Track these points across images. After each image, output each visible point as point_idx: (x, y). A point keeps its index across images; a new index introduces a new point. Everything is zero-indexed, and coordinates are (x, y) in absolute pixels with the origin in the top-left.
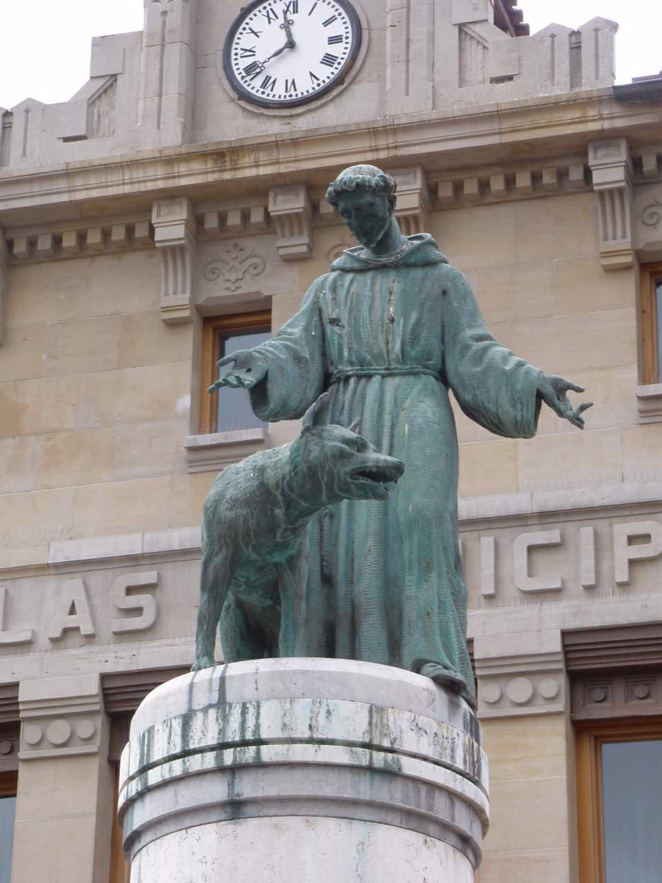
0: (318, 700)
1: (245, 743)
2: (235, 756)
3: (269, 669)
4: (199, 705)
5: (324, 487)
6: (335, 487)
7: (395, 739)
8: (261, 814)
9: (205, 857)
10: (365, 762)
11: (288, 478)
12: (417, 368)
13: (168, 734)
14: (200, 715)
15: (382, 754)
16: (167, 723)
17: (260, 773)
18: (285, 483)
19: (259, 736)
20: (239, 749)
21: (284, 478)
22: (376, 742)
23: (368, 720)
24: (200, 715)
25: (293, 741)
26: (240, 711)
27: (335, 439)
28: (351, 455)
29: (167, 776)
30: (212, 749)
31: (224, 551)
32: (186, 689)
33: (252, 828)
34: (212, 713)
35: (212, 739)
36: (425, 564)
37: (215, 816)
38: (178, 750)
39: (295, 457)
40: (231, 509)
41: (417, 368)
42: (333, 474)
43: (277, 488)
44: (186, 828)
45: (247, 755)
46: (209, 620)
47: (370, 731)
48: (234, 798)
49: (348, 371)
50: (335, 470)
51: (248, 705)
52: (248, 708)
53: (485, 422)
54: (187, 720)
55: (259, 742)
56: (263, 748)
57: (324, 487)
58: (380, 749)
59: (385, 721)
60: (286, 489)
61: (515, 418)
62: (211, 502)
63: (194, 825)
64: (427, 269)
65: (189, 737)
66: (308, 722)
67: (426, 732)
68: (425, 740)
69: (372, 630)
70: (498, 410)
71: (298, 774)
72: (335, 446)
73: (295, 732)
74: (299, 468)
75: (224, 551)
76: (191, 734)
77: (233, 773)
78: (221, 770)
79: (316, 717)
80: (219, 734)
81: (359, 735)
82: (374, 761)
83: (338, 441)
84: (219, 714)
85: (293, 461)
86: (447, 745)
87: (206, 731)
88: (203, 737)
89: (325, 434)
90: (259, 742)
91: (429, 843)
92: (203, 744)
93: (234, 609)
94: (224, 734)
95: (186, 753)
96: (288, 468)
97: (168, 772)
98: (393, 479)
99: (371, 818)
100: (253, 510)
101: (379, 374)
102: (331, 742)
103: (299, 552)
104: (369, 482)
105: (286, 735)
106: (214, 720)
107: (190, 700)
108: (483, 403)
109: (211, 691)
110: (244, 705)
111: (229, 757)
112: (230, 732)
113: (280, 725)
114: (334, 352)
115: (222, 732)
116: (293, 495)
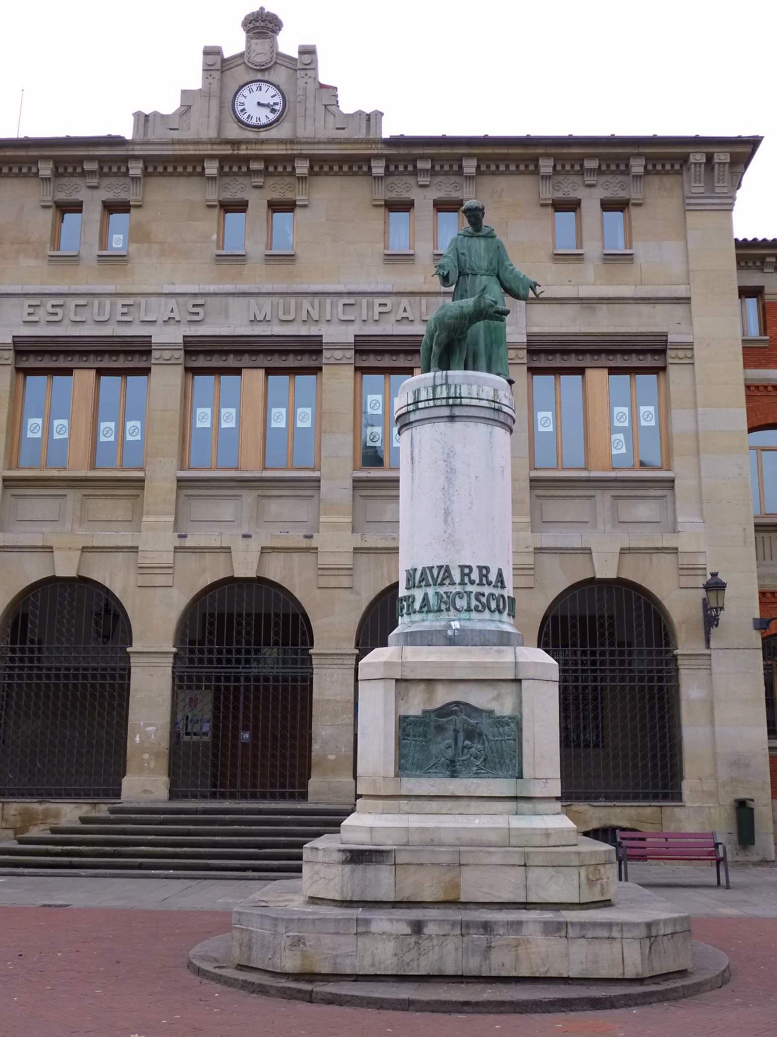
14: (439, 388)
24: (439, 388)
33: (458, 425)
34: (444, 387)
35: (445, 395)
37: (444, 420)
54: (434, 387)
55: (461, 398)
69: (483, 361)
71: (473, 409)
78: (448, 405)
81: (491, 398)
87: (442, 392)
90: (461, 398)
95: (434, 399)
111: (451, 401)
114: (463, 264)
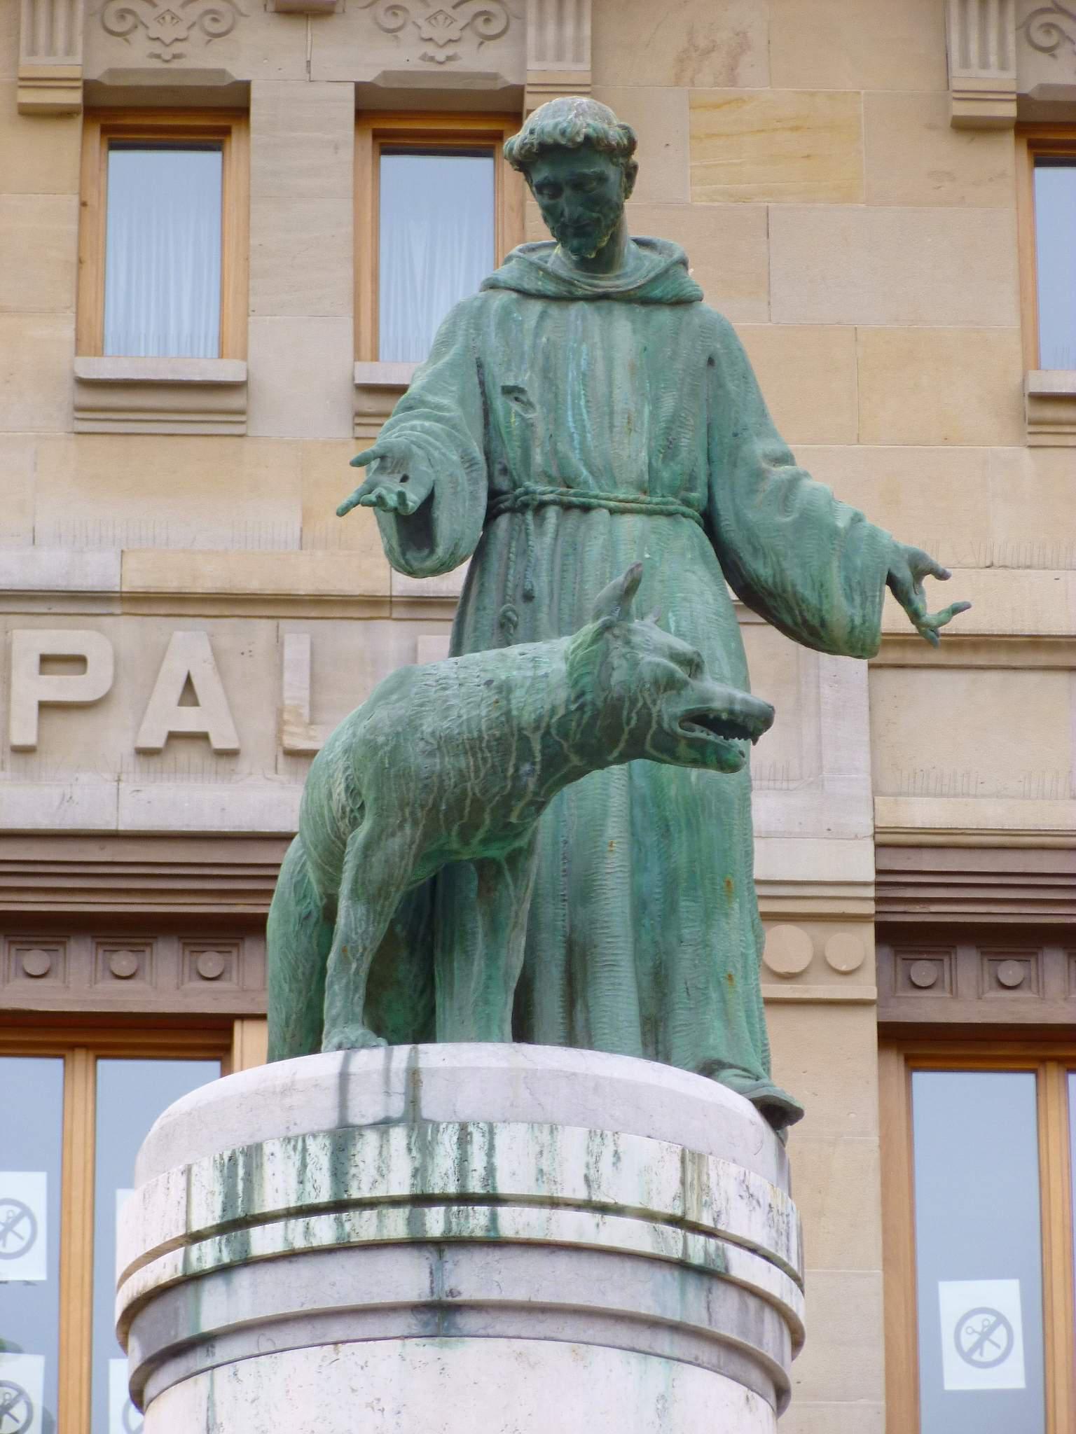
0: (599, 1132)
1: (465, 1199)
2: (448, 1222)
3: (504, 1064)
4: (363, 1116)
5: (625, 736)
6: (649, 737)
7: (719, 1214)
8: (490, 1332)
9: (379, 1400)
10: (677, 1254)
11: (561, 712)
12: (672, 503)
13: (298, 1164)
14: (371, 1138)
15: (702, 1238)
16: (297, 1143)
17: (494, 1256)
18: (554, 720)
19: (494, 1188)
20: (455, 1208)
21: (553, 710)
22: (692, 1217)
23: (678, 1175)
24: (371, 1138)
25: (554, 1203)
26: (455, 1139)
27: (657, 650)
28: (686, 684)
29: (300, 1244)
30: (395, 1202)
31: (408, 829)
32: (333, 1082)
33: (475, 1357)
34: (398, 1136)
35: (400, 1185)
36: (724, 884)
37: (400, 1324)
38: (324, 1196)
39: (581, 676)
40: (431, 754)
41: (672, 503)
42: (650, 715)
43: (537, 728)
44: (336, 1343)
45: (472, 1223)
46: (362, 955)
47: (683, 1196)
48: (444, 1298)
49: (543, 493)
50: (654, 710)
51: (471, 1129)
52: (470, 1134)
53: (788, 620)
54: (343, 1140)
55: (493, 1200)
56: (502, 1211)
57: (625, 736)
58: (696, 1228)
59: (705, 1178)
60: (553, 732)
61: (852, 621)
62: (387, 735)
63: (351, 1338)
64: (680, 311)
65: (350, 1176)
66: (584, 1171)
67: (758, 1202)
68: (759, 1216)
69: (618, 993)
70: (821, 603)
71: (563, 1264)
72: (658, 665)
73: (559, 1187)
74: (588, 697)
75: (408, 829)
76: (353, 1171)
77: (440, 1253)
78: (417, 1243)
79: (596, 1162)
80: (414, 1176)
81: (665, 1204)
82: (690, 1251)
83: (664, 656)
84: (413, 1140)
85: (576, 682)
86: (783, 1227)
87: (386, 1168)
88: (380, 1179)
89: (636, 639)
90: (493, 1200)
91: (752, 1402)
92: (380, 1192)
93: (317, 922)
94: (424, 1178)
95: (339, 1206)
96: (562, 695)
97: (302, 1237)
98: (753, 736)
99: (677, 1353)
100: (480, 762)
101: (605, 507)
102: (618, 1210)
103: (531, 844)
104: (712, 737)
105: (543, 1191)
106: (404, 1150)
107: (343, 1105)
108: (794, 586)
109: (388, 1093)
110: (463, 1128)
111: (435, 1221)
112: (437, 1174)
113: (533, 1172)
114: (512, 453)
115: (419, 1173)
116: (565, 745)
